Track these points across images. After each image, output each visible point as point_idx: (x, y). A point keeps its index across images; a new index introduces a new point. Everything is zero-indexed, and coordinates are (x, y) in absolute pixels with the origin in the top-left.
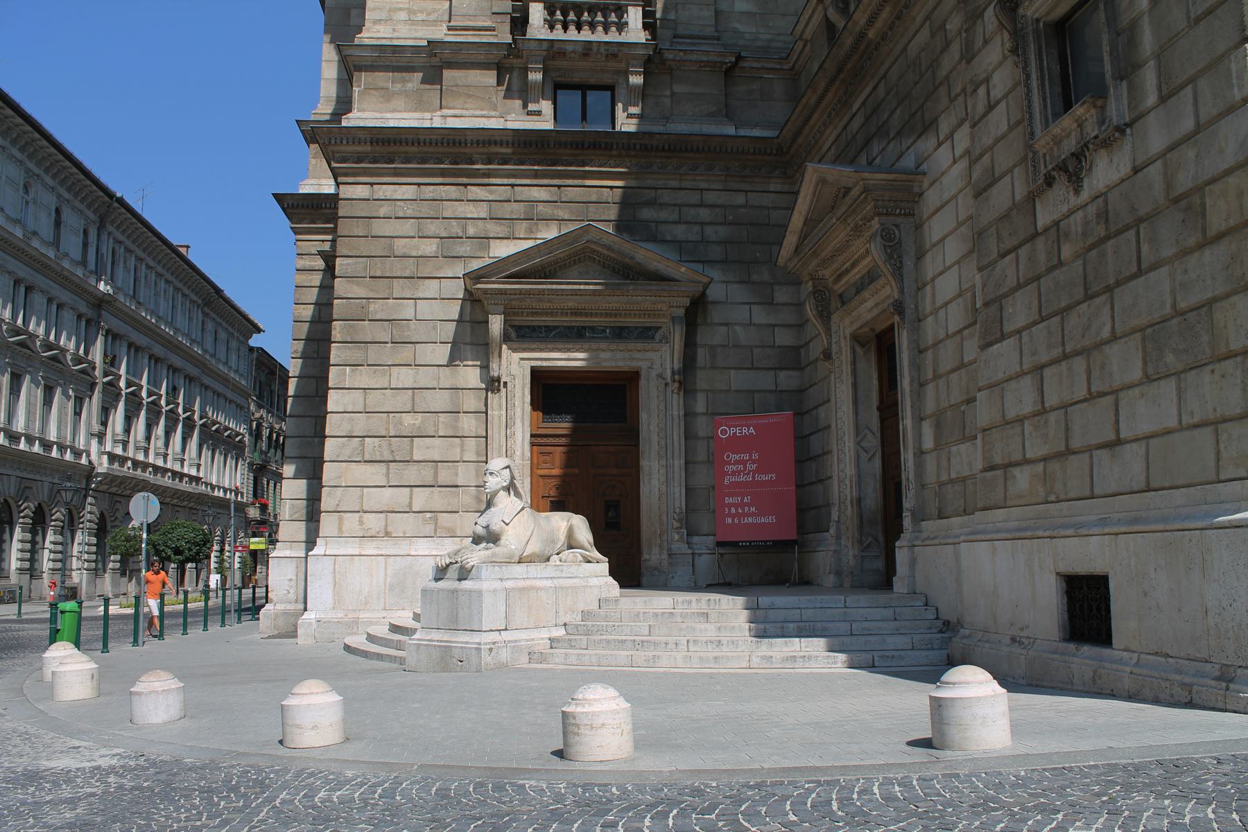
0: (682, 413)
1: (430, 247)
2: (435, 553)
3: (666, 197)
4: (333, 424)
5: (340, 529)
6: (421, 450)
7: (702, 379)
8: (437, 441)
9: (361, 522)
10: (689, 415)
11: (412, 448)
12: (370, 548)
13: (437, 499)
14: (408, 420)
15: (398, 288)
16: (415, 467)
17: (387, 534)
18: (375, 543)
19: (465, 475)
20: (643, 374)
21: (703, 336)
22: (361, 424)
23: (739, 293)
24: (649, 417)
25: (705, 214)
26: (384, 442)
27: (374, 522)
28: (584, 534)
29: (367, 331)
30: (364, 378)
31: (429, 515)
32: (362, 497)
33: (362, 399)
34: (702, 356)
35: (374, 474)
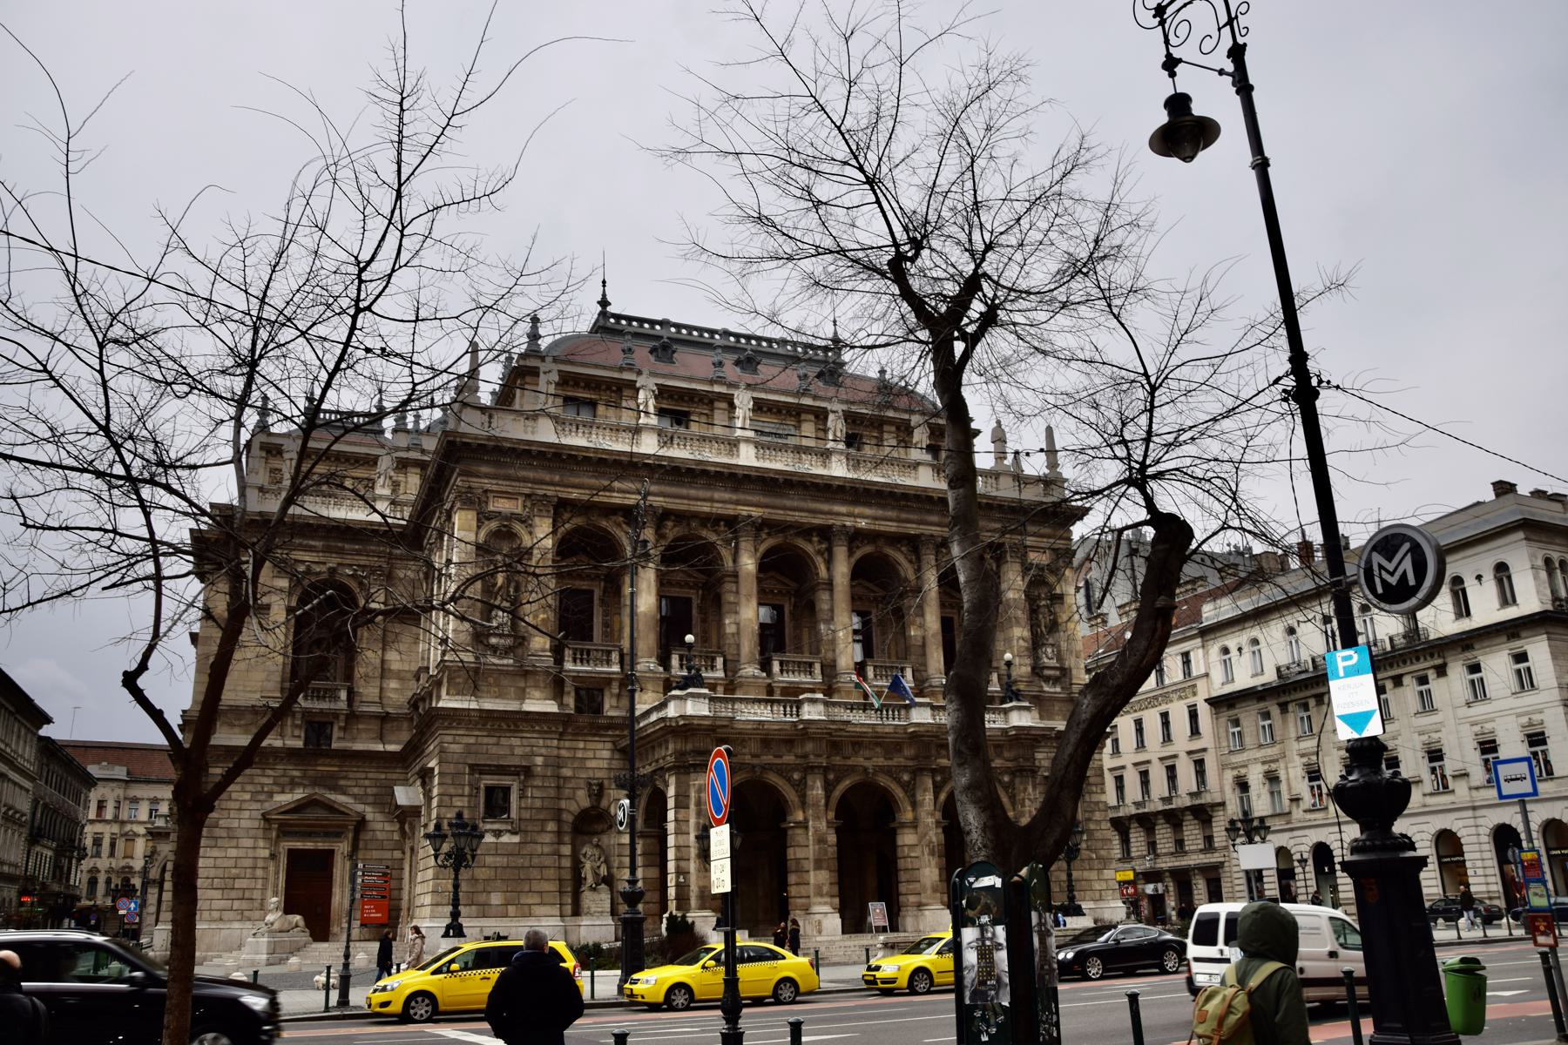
1: (247, 796)
3: (351, 775)
6: (238, 884)
7: (361, 854)
13: (244, 905)
14: (234, 871)
15: (232, 814)
19: (257, 894)
21: (362, 836)
22: (212, 873)
23: (379, 817)
25: (367, 783)
28: (302, 923)
29: (217, 832)
30: (215, 853)
34: (361, 844)
35: (217, 894)
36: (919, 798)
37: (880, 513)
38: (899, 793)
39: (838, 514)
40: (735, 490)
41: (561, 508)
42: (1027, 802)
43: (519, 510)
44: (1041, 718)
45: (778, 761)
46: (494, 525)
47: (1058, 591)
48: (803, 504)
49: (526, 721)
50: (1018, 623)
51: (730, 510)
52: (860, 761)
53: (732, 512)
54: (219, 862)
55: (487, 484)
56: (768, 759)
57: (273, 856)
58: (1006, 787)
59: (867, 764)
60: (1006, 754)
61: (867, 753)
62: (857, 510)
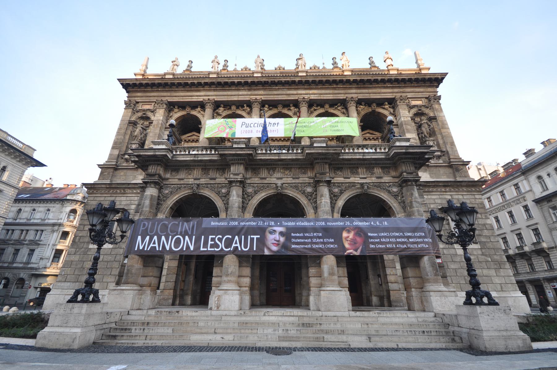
36: (318, 202)
37: (323, 91)
38: (303, 201)
39: (301, 94)
40: (249, 90)
41: (171, 106)
42: (414, 204)
43: (152, 108)
44: (431, 177)
45: (212, 182)
46: (140, 114)
47: (432, 115)
48: (284, 92)
49: (129, 188)
50: (409, 132)
51: (247, 98)
52: (274, 180)
53: (248, 99)
55: (138, 99)
56: (203, 181)
58: (395, 196)
59: (279, 182)
60: (393, 173)
61: (279, 175)
62: (311, 92)
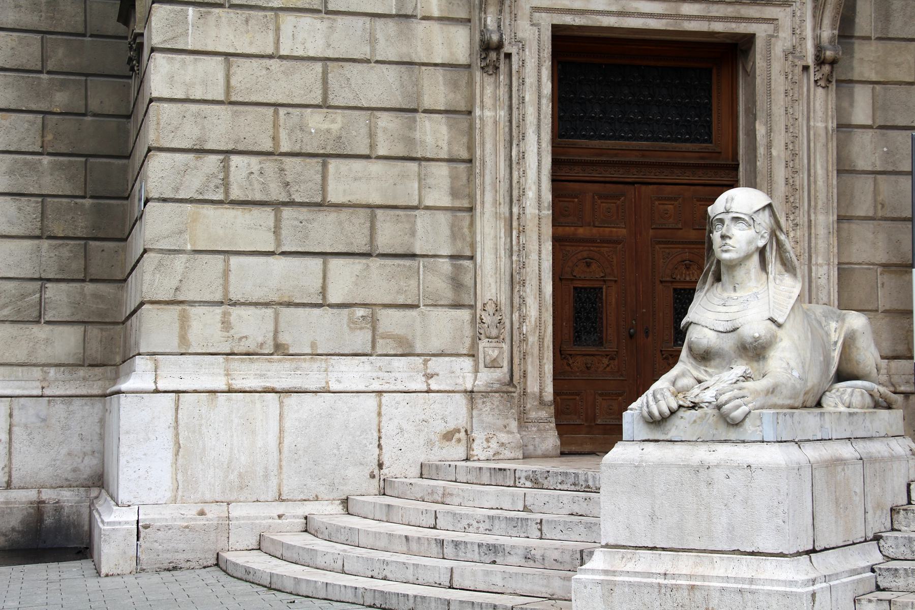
0: (832, 124)
2: (376, 386)
4: (162, 125)
5: (183, 338)
6: (346, 182)
7: (866, 61)
8: (376, 167)
9: (226, 324)
10: (844, 127)
11: (324, 178)
12: (249, 375)
16: (330, 218)
17: (279, 349)
18: (259, 365)
19: (432, 235)
20: (759, 44)
22: (220, 128)
24: (770, 131)
26: (270, 165)
27: (253, 326)
31: (360, 312)
32: (226, 273)
33: (221, 76)
35: (249, 228)
54: (245, 75)
57: (491, 53)
